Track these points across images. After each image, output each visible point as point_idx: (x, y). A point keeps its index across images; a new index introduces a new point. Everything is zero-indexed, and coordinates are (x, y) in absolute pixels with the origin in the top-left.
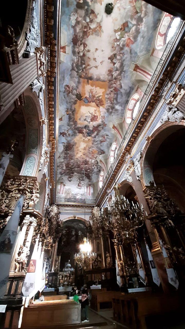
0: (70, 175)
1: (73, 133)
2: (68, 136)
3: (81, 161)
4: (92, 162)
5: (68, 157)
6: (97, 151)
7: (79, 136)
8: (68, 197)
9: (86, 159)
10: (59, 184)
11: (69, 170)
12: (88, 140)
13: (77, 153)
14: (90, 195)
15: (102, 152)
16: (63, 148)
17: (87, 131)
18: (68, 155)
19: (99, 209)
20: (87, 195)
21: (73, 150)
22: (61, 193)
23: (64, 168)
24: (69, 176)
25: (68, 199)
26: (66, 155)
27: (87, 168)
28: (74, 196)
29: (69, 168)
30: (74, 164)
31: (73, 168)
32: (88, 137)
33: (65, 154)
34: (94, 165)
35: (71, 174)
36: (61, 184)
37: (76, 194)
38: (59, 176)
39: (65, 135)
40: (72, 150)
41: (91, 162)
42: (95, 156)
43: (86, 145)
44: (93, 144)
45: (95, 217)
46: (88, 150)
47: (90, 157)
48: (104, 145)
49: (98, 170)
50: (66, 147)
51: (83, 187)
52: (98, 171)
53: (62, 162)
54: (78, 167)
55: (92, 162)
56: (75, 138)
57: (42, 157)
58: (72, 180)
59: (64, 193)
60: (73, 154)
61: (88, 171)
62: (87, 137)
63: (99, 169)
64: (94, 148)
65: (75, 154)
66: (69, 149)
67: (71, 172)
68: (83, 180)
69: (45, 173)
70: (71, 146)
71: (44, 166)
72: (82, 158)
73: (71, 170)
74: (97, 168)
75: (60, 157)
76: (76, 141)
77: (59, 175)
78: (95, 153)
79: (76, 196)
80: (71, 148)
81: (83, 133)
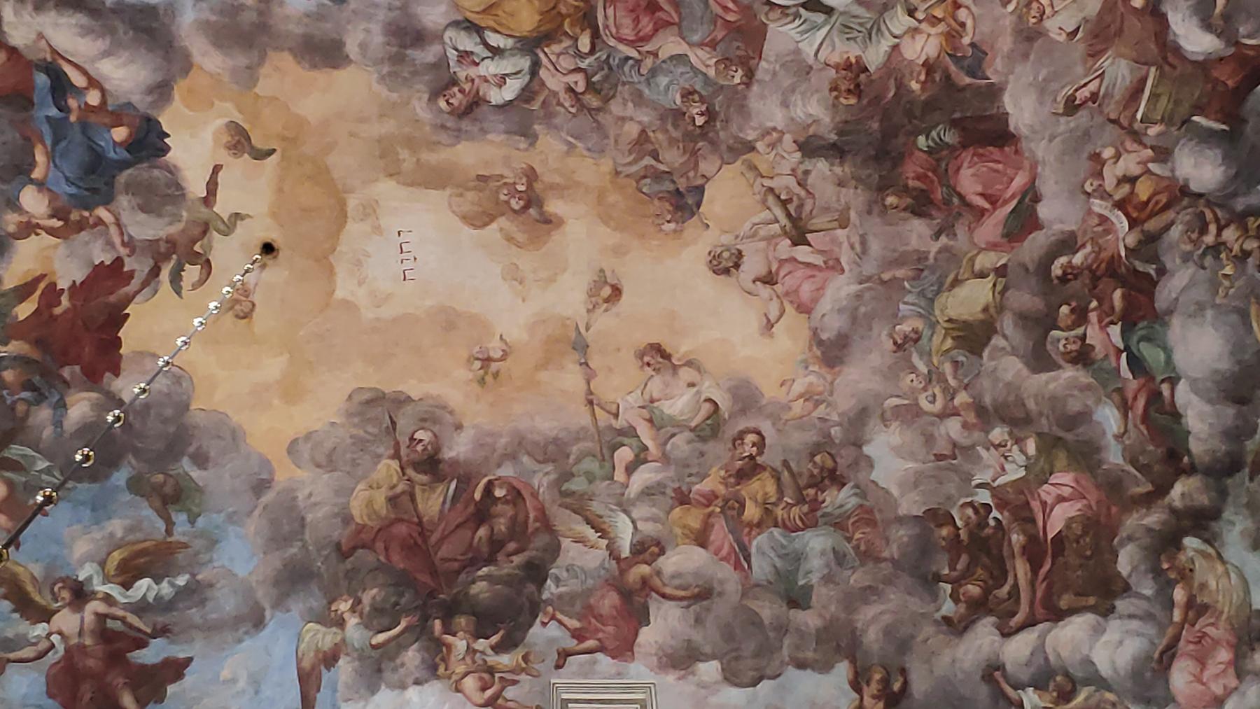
1: (120, 477)
2: (166, 589)
5: (741, 557)
7: (199, 361)
9: (810, 147)
17: (33, 202)
30: (984, 415)
32: (172, 170)
33: (623, 649)
39: (151, 654)
40: (542, 480)
43: (386, 188)
47: (703, 59)
50: (420, 631)
56: (235, 436)
60: (681, 445)
62: (196, 187)
70: (432, 503)
72: (799, 238)
81: (113, 273)
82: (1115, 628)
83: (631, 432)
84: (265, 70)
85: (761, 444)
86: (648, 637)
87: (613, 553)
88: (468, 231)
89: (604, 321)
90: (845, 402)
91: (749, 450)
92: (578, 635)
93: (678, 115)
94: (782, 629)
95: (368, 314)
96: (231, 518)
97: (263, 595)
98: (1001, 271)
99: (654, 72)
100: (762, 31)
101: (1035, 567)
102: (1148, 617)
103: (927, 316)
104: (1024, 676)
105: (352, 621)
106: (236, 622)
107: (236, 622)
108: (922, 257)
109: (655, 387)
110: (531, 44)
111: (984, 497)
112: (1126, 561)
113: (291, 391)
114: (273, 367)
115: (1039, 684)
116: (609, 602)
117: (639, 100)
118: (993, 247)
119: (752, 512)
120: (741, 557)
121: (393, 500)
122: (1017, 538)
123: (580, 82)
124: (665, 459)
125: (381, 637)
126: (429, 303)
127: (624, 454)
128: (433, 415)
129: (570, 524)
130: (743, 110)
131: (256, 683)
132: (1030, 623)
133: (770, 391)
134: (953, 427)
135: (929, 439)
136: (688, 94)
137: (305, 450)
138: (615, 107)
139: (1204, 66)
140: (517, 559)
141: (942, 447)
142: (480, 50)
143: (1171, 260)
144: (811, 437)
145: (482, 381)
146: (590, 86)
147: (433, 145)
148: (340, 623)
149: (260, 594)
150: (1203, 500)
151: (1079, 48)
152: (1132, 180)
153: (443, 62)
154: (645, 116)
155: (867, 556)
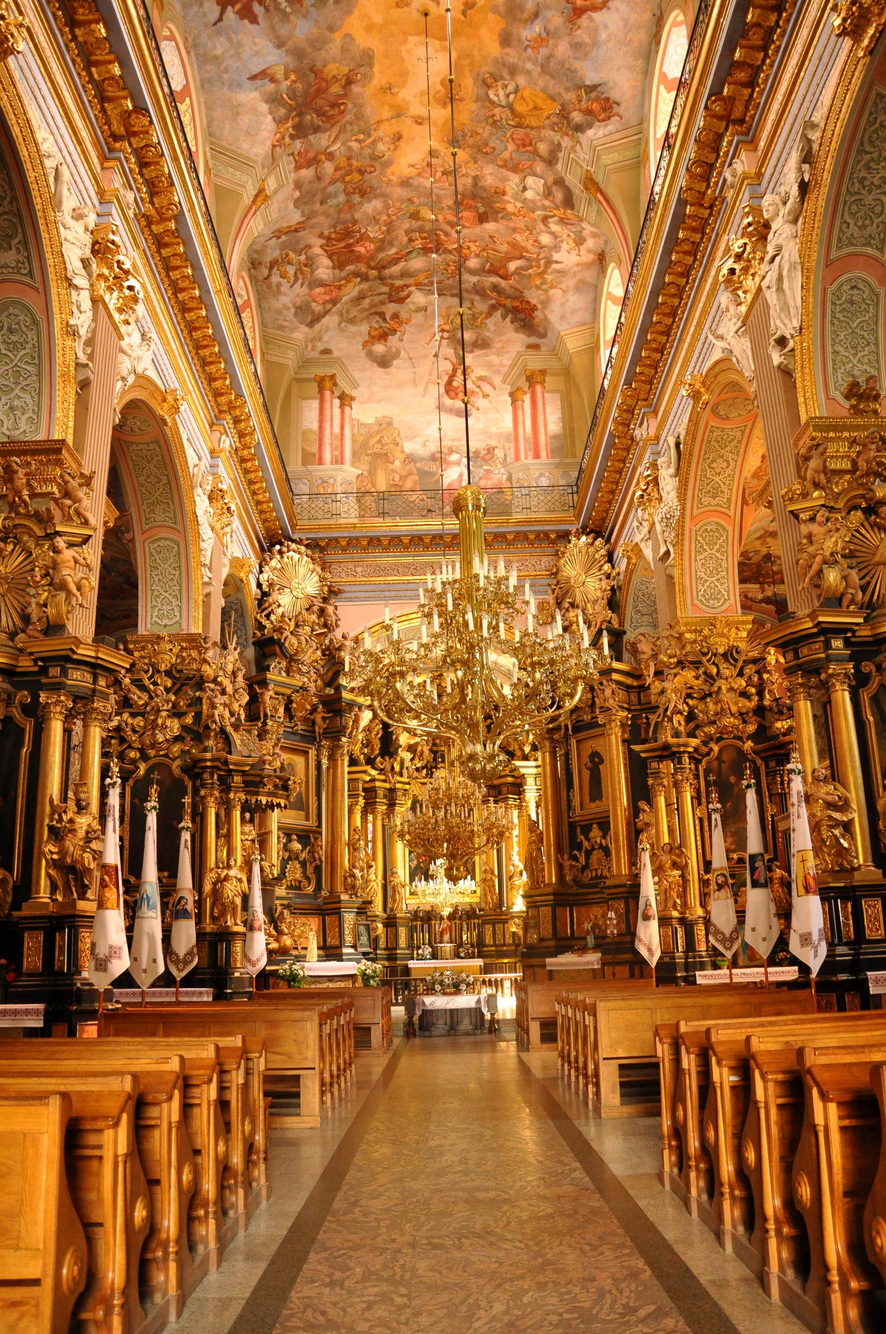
0: (382, 315)
3: (439, 199)
4: (529, 194)
5: (333, 182)
6: (552, 99)
8: (382, 485)
9: (476, 178)
10: (304, 398)
11: (365, 278)
12: (464, 13)
13: (398, 137)
14: (537, 456)
15: (595, 106)
16: (268, 124)
18: (328, 167)
19: (603, 552)
20: (517, 458)
21: (359, 116)
22: (327, 455)
23: (324, 269)
24: (376, 322)
25: (382, 497)
26: (307, 173)
27: (504, 248)
28: (424, 474)
29: (363, 268)
30: (390, 225)
31: (395, 261)
33: (298, 168)
34: (545, 219)
35: (382, 303)
36: (321, 390)
37: (433, 458)
38: (301, 333)
40: (349, 117)
41: (516, 197)
42: (543, 148)
44: (506, 40)
45: (572, 605)
46: (477, 100)
47: (506, 155)
48: (603, 36)
49: (589, 251)
50: (291, 109)
51: (486, 396)
52: (587, 266)
53: (296, 230)
54: (426, 250)
55: (529, 194)
56: (349, 13)
57: (76, 288)
58: (397, 355)
59: (348, 455)
61: (512, 266)
63: (590, 243)
64: (521, 80)
65: (381, 147)
66: (320, 113)
67: (385, 289)
68: (482, 344)
69: (152, 374)
70: (335, 89)
71: (117, 339)
72: (443, 173)
73: (381, 278)
74: (580, 241)
75: (267, 198)
76: (363, 41)
77: (293, 330)
78: (534, 122)
79: (434, 467)
80: (333, 106)
82: (330, 271)
83: (369, 136)
84: (499, 18)
85: (371, 172)
86: (303, 172)
87: (327, 148)
88: (439, 80)
89: (409, 121)
90: (388, 191)
91: (368, 170)
92: (299, 154)
93: (487, 145)
94: (313, 203)
95: (403, 48)
96: (316, 21)
97: (290, 45)
98: (437, 220)
99: (502, 141)
100: (517, 173)
101: (344, 247)
102: (334, 277)
103: (420, 205)
104: (309, 254)
105: (288, 83)
106: (278, 37)
107: (278, 37)
108: (441, 203)
109: (386, 139)
110: (510, 107)
111: (363, 230)
112: (350, 268)
113: (369, 28)
114: (377, 19)
115: (307, 259)
116: (311, 155)
117: (491, 134)
118: (445, 218)
119: (348, 178)
120: (333, 182)
121: (334, 77)
122: (352, 241)
123: (497, 118)
124: (362, 148)
125: (285, 96)
126: (410, 68)
127: (361, 137)
128: (367, 77)
129: (334, 132)
130: (488, 163)
131: (257, 54)
132: (326, 251)
133: (389, 171)
134: (385, 218)
135: (379, 214)
136: (494, 148)
137: (348, 39)
138: (488, 127)
139: (505, 267)
140: (320, 123)
141: (377, 217)
142: (508, 91)
143: (443, 256)
144: (375, 183)
145: (382, 88)
146: (495, 122)
147: (471, 71)
148: (286, 78)
149: (290, 43)
150: (371, 277)
151: (510, 240)
152: (469, 248)
153: (502, 78)
154: (485, 135)
155: (340, 211)
